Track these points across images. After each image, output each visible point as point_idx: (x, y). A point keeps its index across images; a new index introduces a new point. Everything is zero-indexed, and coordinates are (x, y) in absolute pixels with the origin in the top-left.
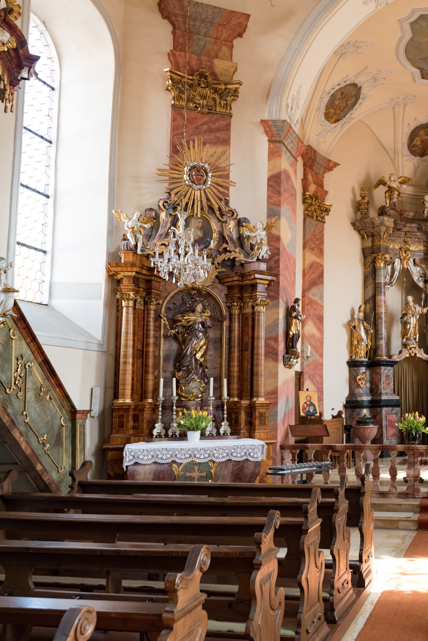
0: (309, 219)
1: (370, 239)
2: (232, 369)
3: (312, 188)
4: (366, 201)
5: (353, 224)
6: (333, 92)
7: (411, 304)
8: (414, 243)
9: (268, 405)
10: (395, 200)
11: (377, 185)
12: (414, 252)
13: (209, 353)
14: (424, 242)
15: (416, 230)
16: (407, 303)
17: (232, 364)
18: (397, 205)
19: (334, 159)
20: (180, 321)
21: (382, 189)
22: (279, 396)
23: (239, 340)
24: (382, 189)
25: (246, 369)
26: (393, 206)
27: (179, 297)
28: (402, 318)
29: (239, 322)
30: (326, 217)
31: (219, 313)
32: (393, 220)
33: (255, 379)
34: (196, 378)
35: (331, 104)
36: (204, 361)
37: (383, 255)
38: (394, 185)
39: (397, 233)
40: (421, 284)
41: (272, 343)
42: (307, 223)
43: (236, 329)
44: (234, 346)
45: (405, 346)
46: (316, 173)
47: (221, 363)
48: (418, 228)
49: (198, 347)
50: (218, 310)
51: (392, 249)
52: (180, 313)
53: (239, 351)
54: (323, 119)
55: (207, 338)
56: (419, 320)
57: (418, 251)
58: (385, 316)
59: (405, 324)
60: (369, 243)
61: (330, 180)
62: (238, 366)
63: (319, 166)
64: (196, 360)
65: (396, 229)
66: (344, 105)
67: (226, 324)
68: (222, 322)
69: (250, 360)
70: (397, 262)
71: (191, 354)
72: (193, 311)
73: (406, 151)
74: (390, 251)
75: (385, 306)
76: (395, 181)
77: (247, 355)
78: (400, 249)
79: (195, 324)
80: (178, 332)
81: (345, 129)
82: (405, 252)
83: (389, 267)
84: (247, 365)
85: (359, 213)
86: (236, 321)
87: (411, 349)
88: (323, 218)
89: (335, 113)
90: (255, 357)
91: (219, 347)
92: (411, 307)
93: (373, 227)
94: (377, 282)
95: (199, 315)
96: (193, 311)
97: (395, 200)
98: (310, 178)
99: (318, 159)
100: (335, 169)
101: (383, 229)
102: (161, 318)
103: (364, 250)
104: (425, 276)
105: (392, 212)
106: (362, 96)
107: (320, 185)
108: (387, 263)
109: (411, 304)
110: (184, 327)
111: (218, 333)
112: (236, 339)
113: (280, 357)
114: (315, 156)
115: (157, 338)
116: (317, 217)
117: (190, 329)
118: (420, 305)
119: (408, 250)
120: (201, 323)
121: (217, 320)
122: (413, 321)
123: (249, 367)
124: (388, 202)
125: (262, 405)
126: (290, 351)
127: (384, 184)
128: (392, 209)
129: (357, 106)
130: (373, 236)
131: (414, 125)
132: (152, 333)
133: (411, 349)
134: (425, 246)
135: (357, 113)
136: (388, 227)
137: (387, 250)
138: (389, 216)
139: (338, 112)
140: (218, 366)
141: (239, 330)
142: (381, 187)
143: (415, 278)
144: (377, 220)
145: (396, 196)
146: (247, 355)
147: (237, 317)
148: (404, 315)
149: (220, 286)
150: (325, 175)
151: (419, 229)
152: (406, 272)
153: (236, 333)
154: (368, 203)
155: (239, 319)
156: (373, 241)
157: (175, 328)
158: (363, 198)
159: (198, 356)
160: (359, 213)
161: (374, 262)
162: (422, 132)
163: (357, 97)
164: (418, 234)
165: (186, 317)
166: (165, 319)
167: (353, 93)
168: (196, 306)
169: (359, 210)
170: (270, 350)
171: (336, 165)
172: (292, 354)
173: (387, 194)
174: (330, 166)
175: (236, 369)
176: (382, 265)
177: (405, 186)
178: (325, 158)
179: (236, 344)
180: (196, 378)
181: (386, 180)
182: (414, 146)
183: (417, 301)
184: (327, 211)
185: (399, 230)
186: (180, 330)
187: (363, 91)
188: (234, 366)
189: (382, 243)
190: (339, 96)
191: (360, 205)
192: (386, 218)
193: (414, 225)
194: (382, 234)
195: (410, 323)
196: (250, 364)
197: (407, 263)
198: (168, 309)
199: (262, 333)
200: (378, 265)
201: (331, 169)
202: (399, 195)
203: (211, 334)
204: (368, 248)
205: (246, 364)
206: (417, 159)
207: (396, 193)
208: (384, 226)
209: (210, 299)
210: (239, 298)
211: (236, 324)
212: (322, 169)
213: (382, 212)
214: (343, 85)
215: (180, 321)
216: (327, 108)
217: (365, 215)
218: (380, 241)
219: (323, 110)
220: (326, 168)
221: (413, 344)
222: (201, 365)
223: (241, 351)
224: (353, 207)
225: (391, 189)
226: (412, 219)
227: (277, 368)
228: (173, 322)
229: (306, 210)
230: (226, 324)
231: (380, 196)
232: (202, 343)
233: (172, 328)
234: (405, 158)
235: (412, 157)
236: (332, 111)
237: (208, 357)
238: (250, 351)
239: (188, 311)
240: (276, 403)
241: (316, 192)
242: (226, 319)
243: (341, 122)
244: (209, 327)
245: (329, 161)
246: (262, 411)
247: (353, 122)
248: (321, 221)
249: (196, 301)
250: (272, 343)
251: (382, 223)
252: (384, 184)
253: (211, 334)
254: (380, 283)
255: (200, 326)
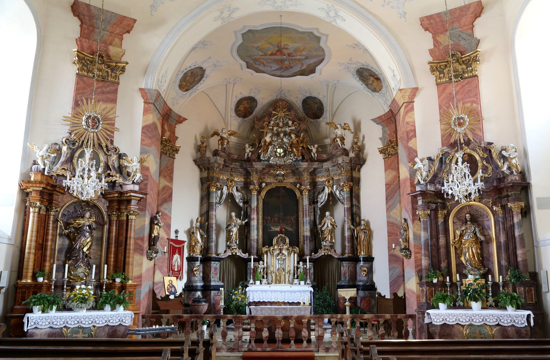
0: (164, 156)
1: (206, 172)
2: (109, 260)
3: (168, 134)
4: (205, 145)
5: (195, 161)
6: (185, 71)
7: (234, 218)
8: (237, 176)
9: (135, 286)
10: (225, 146)
11: (213, 135)
12: (237, 182)
13: (93, 248)
14: (244, 175)
15: (238, 167)
16: (231, 217)
17: (109, 256)
18: (226, 149)
19: (184, 116)
20: (72, 224)
21: (216, 138)
22: (143, 280)
23: (115, 239)
24: (216, 138)
25: (120, 260)
26: (224, 150)
27: (72, 207)
28: (227, 227)
29: (116, 226)
30: (176, 155)
31: (101, 219)
32: (223, 159)
33: (127, 267)
34: (82, 265)
35: (184, 79)
36: (89, 253)
37: (215, 183)
38: (225, 136)
39: (226, 168)
40: (241, 204)
41: (139, 242)
42: (162, 159)
43: (114, 231)
44: (112, 244)
45: (229, 247)
46: (170, 124)
47: (101, 255)
48: (240, 166)
49: (86, 243)
50: (100, 217)
51: (222, 180)
52: (73, 218)
53: (115, 247)
54: (178, 88)
55: (92, 236)
56: (239, 229)
57: (240, 182)
58: (216, 226)
59: (229, 232)
60: (205, 175)
61: (180, 130)
62: (114, 258)
63: (172, 120)
64: (83, 252)
65: (225, 166)
66: (192, 80)
67: (106, 227)
68: (103, 226)
69: (123, 254)
70: (225, 188)
71: (80, 247)
72: (83, 217)
73: (234, 114)
74: (220, 181)
75: (215, 219)
76: (225, 133)
77: (122, 249)
78: (228, 179)
79: (84, 226)
80: (70, 232)
81: (192, 96)
82: (231, 182)
83: (219, 192)
84: (121, 257)
85: (199, 153)
86: (114, 225)
87: (233, 249)
88: (174, 155)
89: (186, 85)
90: (127, 251)
91: (100, 244)
92: (233, 221)
93: (209, 164)
94: (210, 201)
95: (87, 220)
96: (83, 217)
97: (225, 146)
98: (166, 127)
99: (172, 115)
100: (184, 122)
101: (216, 165)
102: (58, 221)
103: (201, 179)
104: (244, 199)
105: (222, 154)
106: (205, 76)
107: (173, 132)
108: (218, 189)
109: (234, 218)
110: (75, 228)
111: (100, 233)
112: (114, 238)
113: (145, 252)
114: (171, 113)
115: (54, 236)
116: (170, 154)
117: (79, 230)
118: (240, 219)
119: (233, 180)
120: (88, 226)
121: (100, 224)
122: (235, 230)
123: (123, 258)
124: (220, 147)
125: (131, 286)
126: (152, 247)
127: (218, 135)
128: (222, 152)
129: (201, 82)
130: (208, 169)
131: (239, 97)
132: (51, 232)
133: (233, 249)
134: (244, 178)
135: (201, 86)
136: (219, 164)
137: (218, 180)
138: (221, 156)
139: (188, 84)
140: (99, 257)
141: (116, 232)
142: (216, 136)
143: (237, 201)
144: (213, 159)
145: (226, 143)
146: (122, 249)
147: (115, 222)
148: (228, 226)
149: (103, 200)
150: (177, 126)
151: (241, 166)
152: (231, 196)
153: (114, 234)
154: (206, 147)
155: (116, 224)
156: (208, 173)
157: (68, 229)
158: (203, 143)
159: (85, 249)
160: (199, 153)
161: (208, 188)
162: (245, 102)
163: (202, 76)
164: (240, 170)
165: (78, 222)
166: (61, 222)
167: (200, 73)
168: (85, 214)
169: (199, 151)
170: (138, 247)
171: (185, 119)
172: (153, 250)
173: (220, 142)
174: (181, 120)
175: (112, 260)
176: (214, 190)
177: (232, 137)
178: (177, 115)
179: (113, 242)
180: (82, 265)
181: (219, 132)
182: (239, 110)
183: (238, 216)
184: (177, 151)
185: (227, 166)
186: (73, 230)
187: (207, 72)
188: (111, 258)
189: (215, 175)
190: (190, 74)
191: (200, 148)
192: (218, 158)
193: (238, 164)
194: (215, 168)
195: (232, 232)
196: (123, 256)
197: (232, 189)
198: (64, 215)
199: (132, 234)
200: (211, 190)
201: (180, 122)
202: (228, 142)
203: (95, 233)
204: (205, 178)
205: (120, 256)
206: (240, 119)
207: (226, 141)
208: (217, 163)
209: (95, 209)
210: (117, 209)
211: (114, 228)
212: (175, 122)
213: (216, 153)
214: (193, 67)
215: (72, 224)
216: (181, 81)
217: (203, 155)
218: (213, 173)
219: (178, 83)
220: (177, 121)
221: (234, 246)
222: (87, 256)
223: (117, 247)
224: (195, 148)
225: (222, 139)
226: (236, 159)
227: (142, 260)
228: (67, 225)
229: (162, 149)
230: (106, 227)
231: (214, 143)
232: (89, 240)
233: (66, 229)
234: (233, 118)
235: (238, 118)
236: (184, 84)
237: (91, 251)
238: (123, 247)
239: (79, 217)
240: (141, 285)
241: (170, 137)
242: (106, 224)
243: (190, 91)
244: (94, 229)
245: (180, 116)
246: (131, 290)
247: (198, 92)
248: (172, 158)
249: (85, 210)
250: (139, 242)
251: (216, 162)
252: (218, 135)
253: (95, 233)
254: (213, 202)
255: (88, 228)
